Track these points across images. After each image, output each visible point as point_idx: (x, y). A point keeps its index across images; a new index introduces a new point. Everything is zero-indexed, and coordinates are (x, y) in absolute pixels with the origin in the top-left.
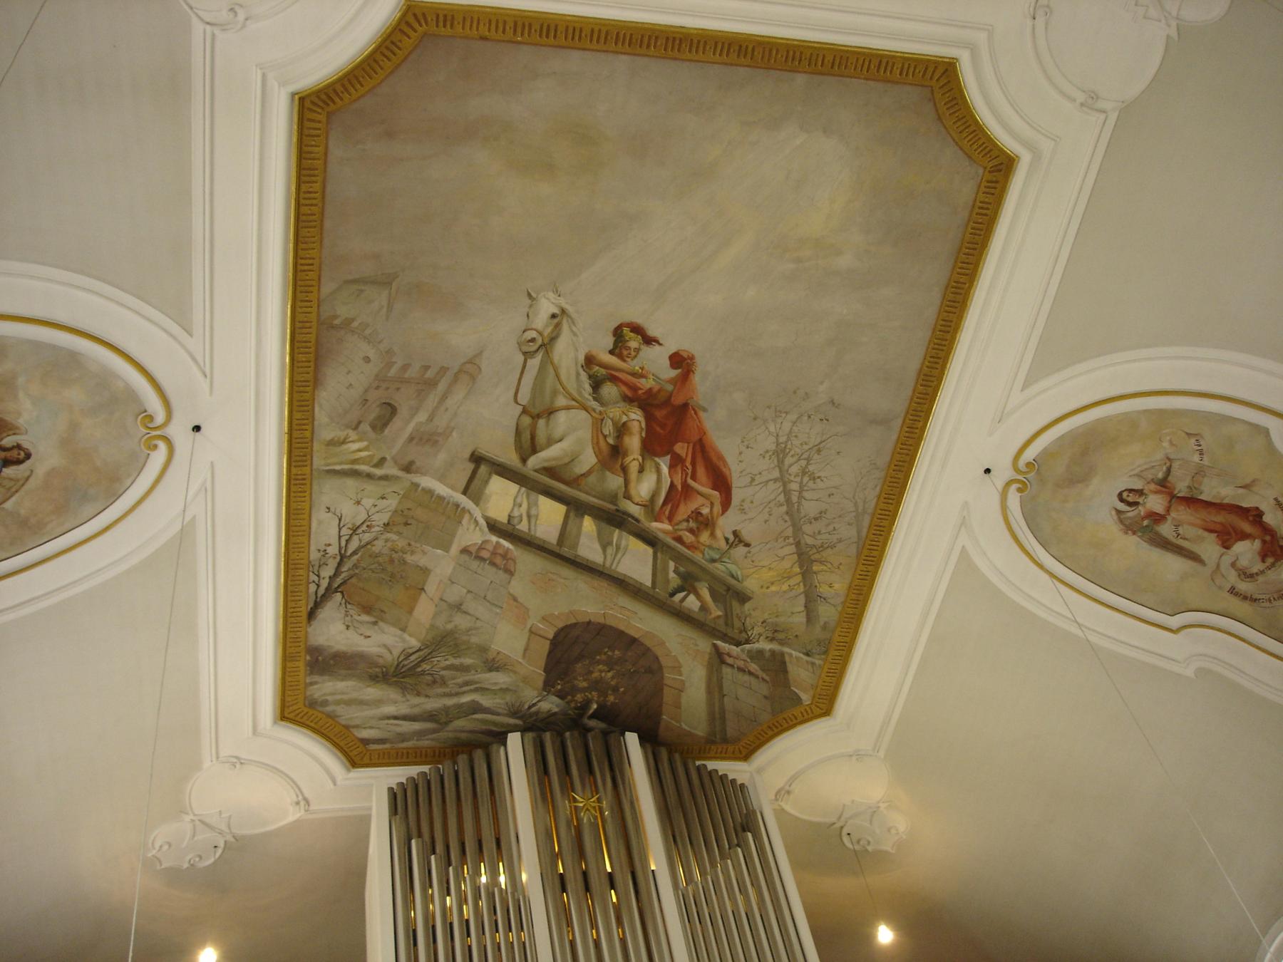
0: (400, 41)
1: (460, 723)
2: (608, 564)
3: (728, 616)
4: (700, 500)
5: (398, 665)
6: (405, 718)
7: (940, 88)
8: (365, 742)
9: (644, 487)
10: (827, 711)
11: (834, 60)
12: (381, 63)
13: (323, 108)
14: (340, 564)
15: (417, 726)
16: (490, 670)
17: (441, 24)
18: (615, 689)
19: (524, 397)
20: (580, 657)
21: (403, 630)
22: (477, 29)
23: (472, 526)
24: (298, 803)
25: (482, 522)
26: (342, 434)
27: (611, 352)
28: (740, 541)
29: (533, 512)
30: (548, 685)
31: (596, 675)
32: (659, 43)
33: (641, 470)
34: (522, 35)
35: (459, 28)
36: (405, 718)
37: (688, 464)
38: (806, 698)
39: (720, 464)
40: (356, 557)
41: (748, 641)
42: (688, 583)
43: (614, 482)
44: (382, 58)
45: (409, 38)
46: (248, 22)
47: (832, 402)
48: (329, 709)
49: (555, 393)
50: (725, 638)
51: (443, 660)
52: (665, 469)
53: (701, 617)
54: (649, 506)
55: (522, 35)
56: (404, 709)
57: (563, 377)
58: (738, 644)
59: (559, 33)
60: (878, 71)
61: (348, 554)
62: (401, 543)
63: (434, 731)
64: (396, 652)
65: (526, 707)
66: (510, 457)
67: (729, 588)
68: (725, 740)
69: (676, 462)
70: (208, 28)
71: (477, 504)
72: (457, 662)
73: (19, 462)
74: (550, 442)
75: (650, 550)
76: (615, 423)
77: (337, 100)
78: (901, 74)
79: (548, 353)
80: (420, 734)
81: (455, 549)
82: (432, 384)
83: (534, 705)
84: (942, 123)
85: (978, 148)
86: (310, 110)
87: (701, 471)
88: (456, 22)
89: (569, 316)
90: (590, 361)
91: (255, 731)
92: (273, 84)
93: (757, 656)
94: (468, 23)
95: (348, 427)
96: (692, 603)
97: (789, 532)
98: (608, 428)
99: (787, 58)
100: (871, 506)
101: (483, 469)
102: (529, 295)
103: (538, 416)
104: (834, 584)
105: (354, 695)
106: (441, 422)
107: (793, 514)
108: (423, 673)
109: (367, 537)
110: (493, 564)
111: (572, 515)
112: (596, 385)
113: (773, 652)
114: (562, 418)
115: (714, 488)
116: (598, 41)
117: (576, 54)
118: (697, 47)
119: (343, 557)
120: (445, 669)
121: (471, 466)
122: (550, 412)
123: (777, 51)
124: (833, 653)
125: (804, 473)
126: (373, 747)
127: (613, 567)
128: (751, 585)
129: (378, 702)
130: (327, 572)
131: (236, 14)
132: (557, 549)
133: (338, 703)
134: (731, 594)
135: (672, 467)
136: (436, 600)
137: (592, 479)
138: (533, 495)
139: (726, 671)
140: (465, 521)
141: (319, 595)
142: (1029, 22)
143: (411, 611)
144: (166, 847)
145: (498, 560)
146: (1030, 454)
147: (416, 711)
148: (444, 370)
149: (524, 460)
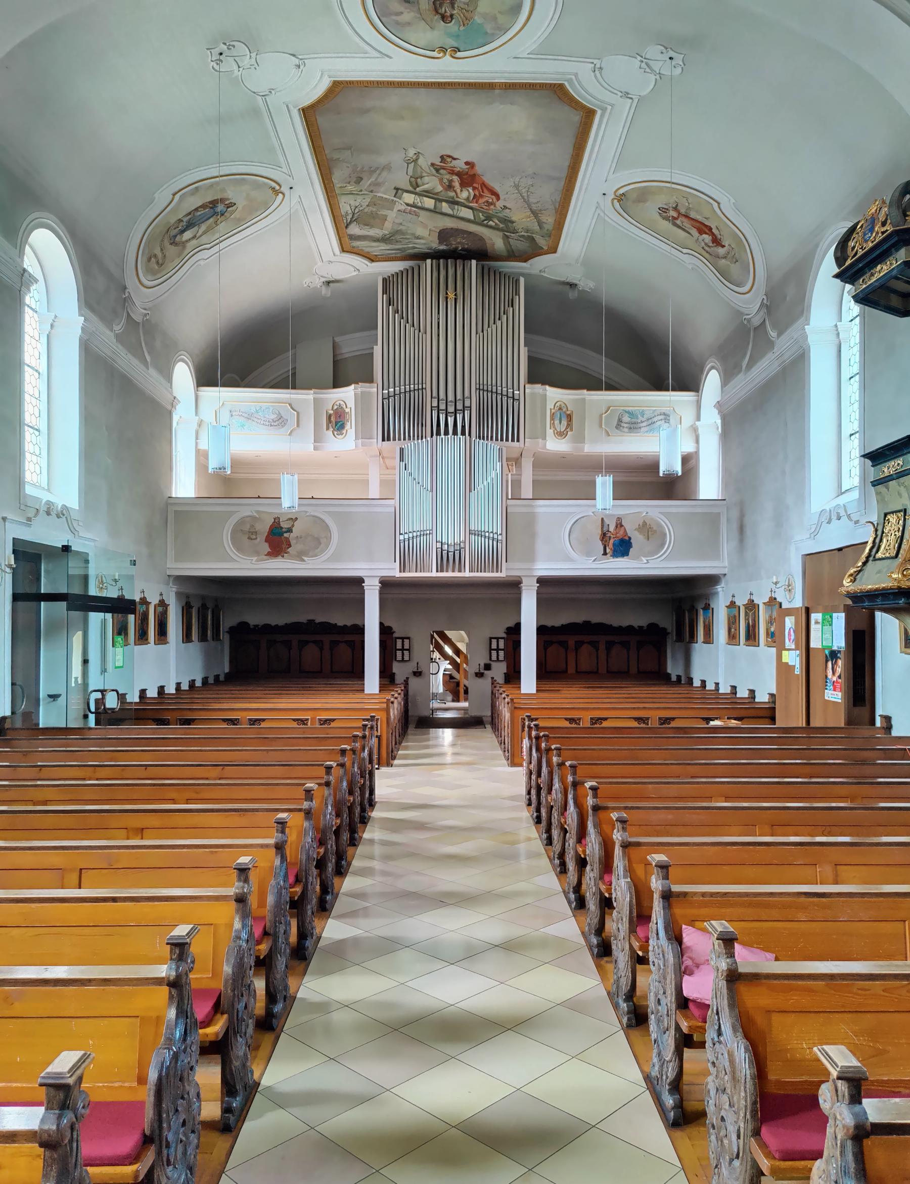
2: (455, 214)
3: (507, 226)
4: (487, 198)
6: (388, 250)
8: (376, 255)
9: (465, 194)
10: (555, 252)
14: (353, 215)
16: (417, 239)
18: (467, 244)
19: (410, 172)
20: (451, 237)
26: (345, 185)
28: (507, 208)
29: (422, 201)
30: (440, 243)
31: (458, 241)
33: (461, 191)
36: (388, 250)
37: (480, 188)
38: (545, 248)
41: (517, 233)
42: (489, 218)
43: (452, 194)
47: (535, 174)
49: (422, 172)
50: (507, 232)
51: (398, 237)
53: (497, 227)
54: (468, 199)
56: (388, 248)
57: (423, 167)
58: (513, 233)
66: (411, 189)
67: (506, 220)
68: (515, 256)
69: (474, 188)
72: (404, 237)
74: (423, 184)
75: (471, 211)
76: (448, 180)
79: (415, 162)
80: (395, 253)
81: (395, 210)
82: (375, 171)
87: (485, 190)
89: (421, 154)
90: (433, 165)
91: (334, 255)
93: (523, 236)
95: (346, 183)
96: (491, 223)
97: (526, 206)
98: (445, 181)
100: (559, 200)
101: (400, 191)
102: (404, 149)
103: (417, 178)
104: (549, 220)
106: (380, 180)
107: (526, 202)
110: (410, 214)
111: (437, 202)
112: (437, 171)
113: (528, 236)
114: (426, 179)
115: (492, 195)
119: (354, 214)
121: (395, 191)
122: (421, 177)
124: (552, 237)
125: (528, 191)
128: (514, 219)
129: (378, 247)
134: (507, 221)
135: (473, 190)
136: (392, 222)
137: (442, 193)
138: (421, 197)
139: (510, 240)
142: (592, 74)
143: (383, 225)
145: (412, 213)
146: (621, 191)
148: (378, 168)
149: (415, 189)
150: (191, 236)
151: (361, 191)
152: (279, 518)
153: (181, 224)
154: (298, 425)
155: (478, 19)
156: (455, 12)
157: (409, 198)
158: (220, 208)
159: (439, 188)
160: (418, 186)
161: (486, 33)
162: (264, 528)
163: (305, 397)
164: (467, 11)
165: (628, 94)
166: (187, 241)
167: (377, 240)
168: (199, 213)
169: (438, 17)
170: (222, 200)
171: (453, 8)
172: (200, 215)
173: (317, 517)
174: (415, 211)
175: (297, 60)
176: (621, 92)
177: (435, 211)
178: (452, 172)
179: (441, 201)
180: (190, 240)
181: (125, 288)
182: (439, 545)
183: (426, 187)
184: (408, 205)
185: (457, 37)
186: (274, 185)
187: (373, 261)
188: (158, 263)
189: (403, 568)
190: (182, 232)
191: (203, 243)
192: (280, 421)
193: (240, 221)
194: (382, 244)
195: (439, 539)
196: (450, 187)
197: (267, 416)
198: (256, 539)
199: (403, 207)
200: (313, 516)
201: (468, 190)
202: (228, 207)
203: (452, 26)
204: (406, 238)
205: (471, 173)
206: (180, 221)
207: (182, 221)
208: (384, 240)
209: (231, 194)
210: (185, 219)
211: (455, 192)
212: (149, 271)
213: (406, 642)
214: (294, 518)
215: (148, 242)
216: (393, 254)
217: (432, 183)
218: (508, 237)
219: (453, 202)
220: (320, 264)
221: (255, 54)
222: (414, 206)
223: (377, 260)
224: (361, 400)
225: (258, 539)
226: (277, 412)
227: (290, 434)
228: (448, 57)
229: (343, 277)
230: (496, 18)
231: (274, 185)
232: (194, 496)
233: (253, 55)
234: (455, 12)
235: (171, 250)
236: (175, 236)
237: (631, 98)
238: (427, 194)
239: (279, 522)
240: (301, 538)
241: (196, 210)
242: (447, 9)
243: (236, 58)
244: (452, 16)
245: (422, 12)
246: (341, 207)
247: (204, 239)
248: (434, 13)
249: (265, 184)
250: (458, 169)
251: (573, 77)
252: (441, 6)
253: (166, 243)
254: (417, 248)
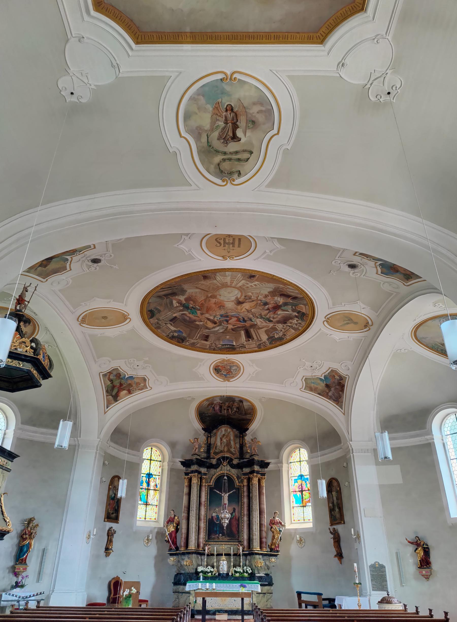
0: (326, 30)
7: (137, 32)
11: (178, 38)
12: (333, 22)
13: (356, 5)
17: (312, 37)
22: (300, 36)
32: (240, 37)
34: (285, 35)
35: (306, 36)
44: (332, 24)
45: (323, 31)
46: (374, 38)
55: (285, 35)
59: (273, 37)
60: (161, 35)
70: (387, 37)
77: (350, 8)
78: (153, 36)
84: (130, 19)
85: (111, 12)
86: (360, 4)
88: (307, 37)
92: (371, 16)
94: (303, 38)
99: (195, 37)
116: (260, 36)
117: (267, 30)
118: (226, 37)
123: (199, 39)
131: (377, 42)
155: (210, 108)
156: (224, 113)
161: (203, 96)
164: (217, 114)
169: (235, 110)
171: (226, 117)
175: (340, 73)
185: (223, 92)
203: (226, 101)
213: (304, 597)
221: (366, 87)
228: (229, 73)
230: (199, 109)
234: (224, 113)
242: (229, 115)
244: (227, 111)
245: (245, 114)
248: (237, 113)
251: (130, 53)
252: (233, 118)
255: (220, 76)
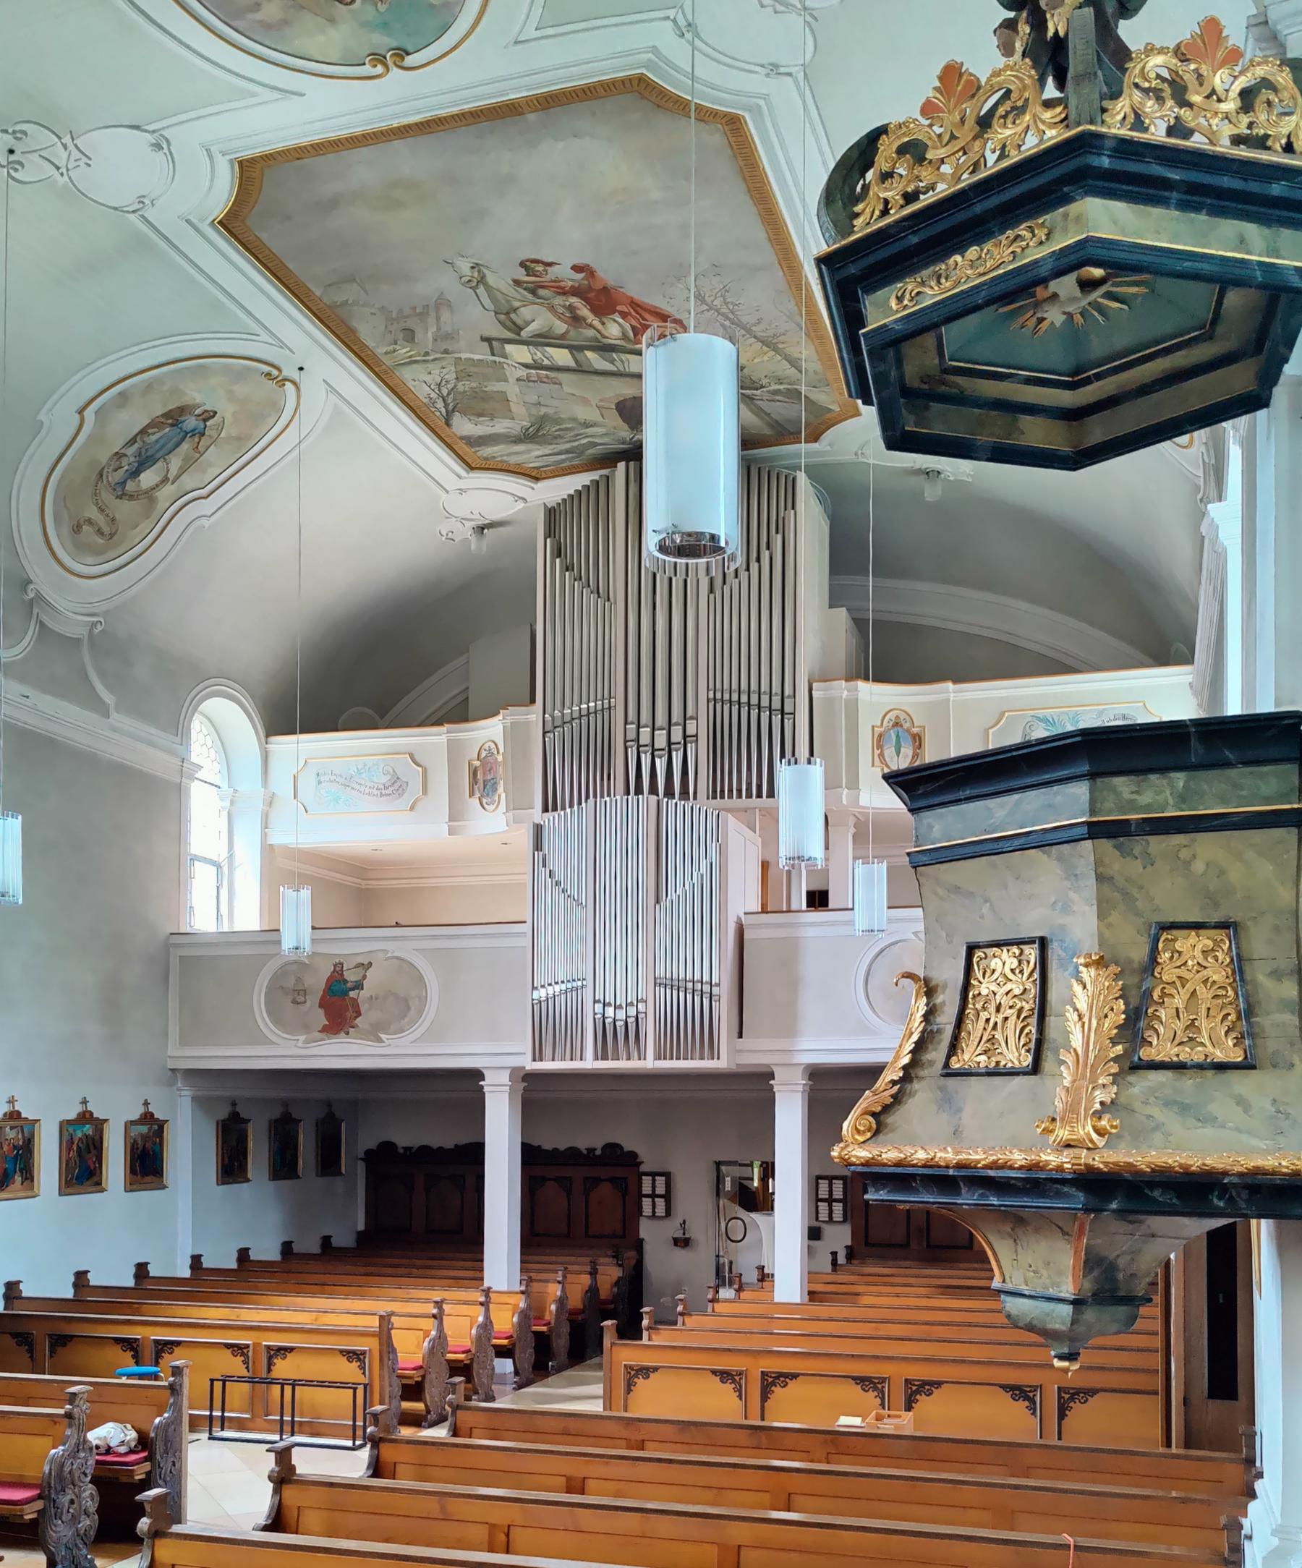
1: (590, 451)
5: (524, 434)
8: (538, 468)
15: (563, 457)
16: (587, 427)
21: (513, 419)
23: (513, 369)
24: (516, 501)
25: (517, 365)
27: (528, 275)
29: (547, 355)
33: (603, 324)
37: (634, 313)
39: (658, 310)
40: (452, 396)
48: (499, 459)
52: (620, 320)
56: (547, 452)
61: (445, 395)
62: (474, 385)
63: (577, 457)
64: (519, 430)
65: (628, 439)
69: (624, 315)
71: (507, 359)
73: (213, 417)
80: (570, 460)
83: (633, 438)
87: (647, 316)
91: (460, 477)
105: (509, 451)
108: (544, 435)
109: (450, 386)
120: (556, 431)
126: (542, 469)
127: (627, 370)
129: (529, 451)
130: (440, 404)
132: (577, 368)
133: (501, 456)
140: (505, 367)
141: (445, 415)
143: (510, 411)
144: (450, 534)
145: (545, 380)
147: (555, 451)
150: (157, 479)
151: (427, 354)
152: (342, 964)
153: (124, 461)
154: (425, 791)
157: (520, 354)
158: (191, 422)
159: (561, 327)
160: (521, 329)
162: (317, 983)
163: (433, 740)
165: (776, 66)
166: (155, 488)
167: (518, 440)
168: (153, 438)
170: (182, 410)
172: (157, 441)
173: (403, 960)
174: (547, 377)
176: (762, 66)
177: (581, 369)
178: (563, 292)
179: (581, 349)
180: (157, 486)
181: (29, 582)
182: (599, 1007)
183: (533, 328)
184: (526, 366)
186: (266, 368)
187: (537, 479)
188: (100, 532)
189: (538, 1055)
190: (135, 474)
191: (189, 488)
192: (396, 786)
193: (242, 441)
194: (530, 446)
195: (599, 996)
196: (576, 320)
197: (375, 779)
198: (305, 1002)
199: (522, 373)
200: (397, 958)
201: (615, 321)
202: (205, 420)
204: (566, 429)
205: (598, 286)
206: (119, 455)
207: (125, 455)
208: (528, 437)
209: (198, 395)
210: (131, 451)
211: (591, 326)
212: (81, 548)
214: (366, 963)
215: (63, 498)
216: (563, 461)
217: (538, 318)
218: (750, 398)
219: (606, 349)
220: (444, 495)
222: (537, 366)
223: (544, 476)
224: (513, 733)
225: (309, 1003)
226: (392, 771)
227: (412, 809)
229: (510, 512)
231: (266, 368)
232: (259, 929)
233: (67, 140)
235: (123, 509)
236: (124, 483)
237: (790, 74)
238: (544, 339)
239: (342, 970)
240: (376, 998)
241: (143, 432)
243: (44, 153)
246: (411, 388)
247: (188, 481)
249: (249, 369)
250: (570, 283)
253: (107, 497)
254: (601, 444)
255: (410, 61)
